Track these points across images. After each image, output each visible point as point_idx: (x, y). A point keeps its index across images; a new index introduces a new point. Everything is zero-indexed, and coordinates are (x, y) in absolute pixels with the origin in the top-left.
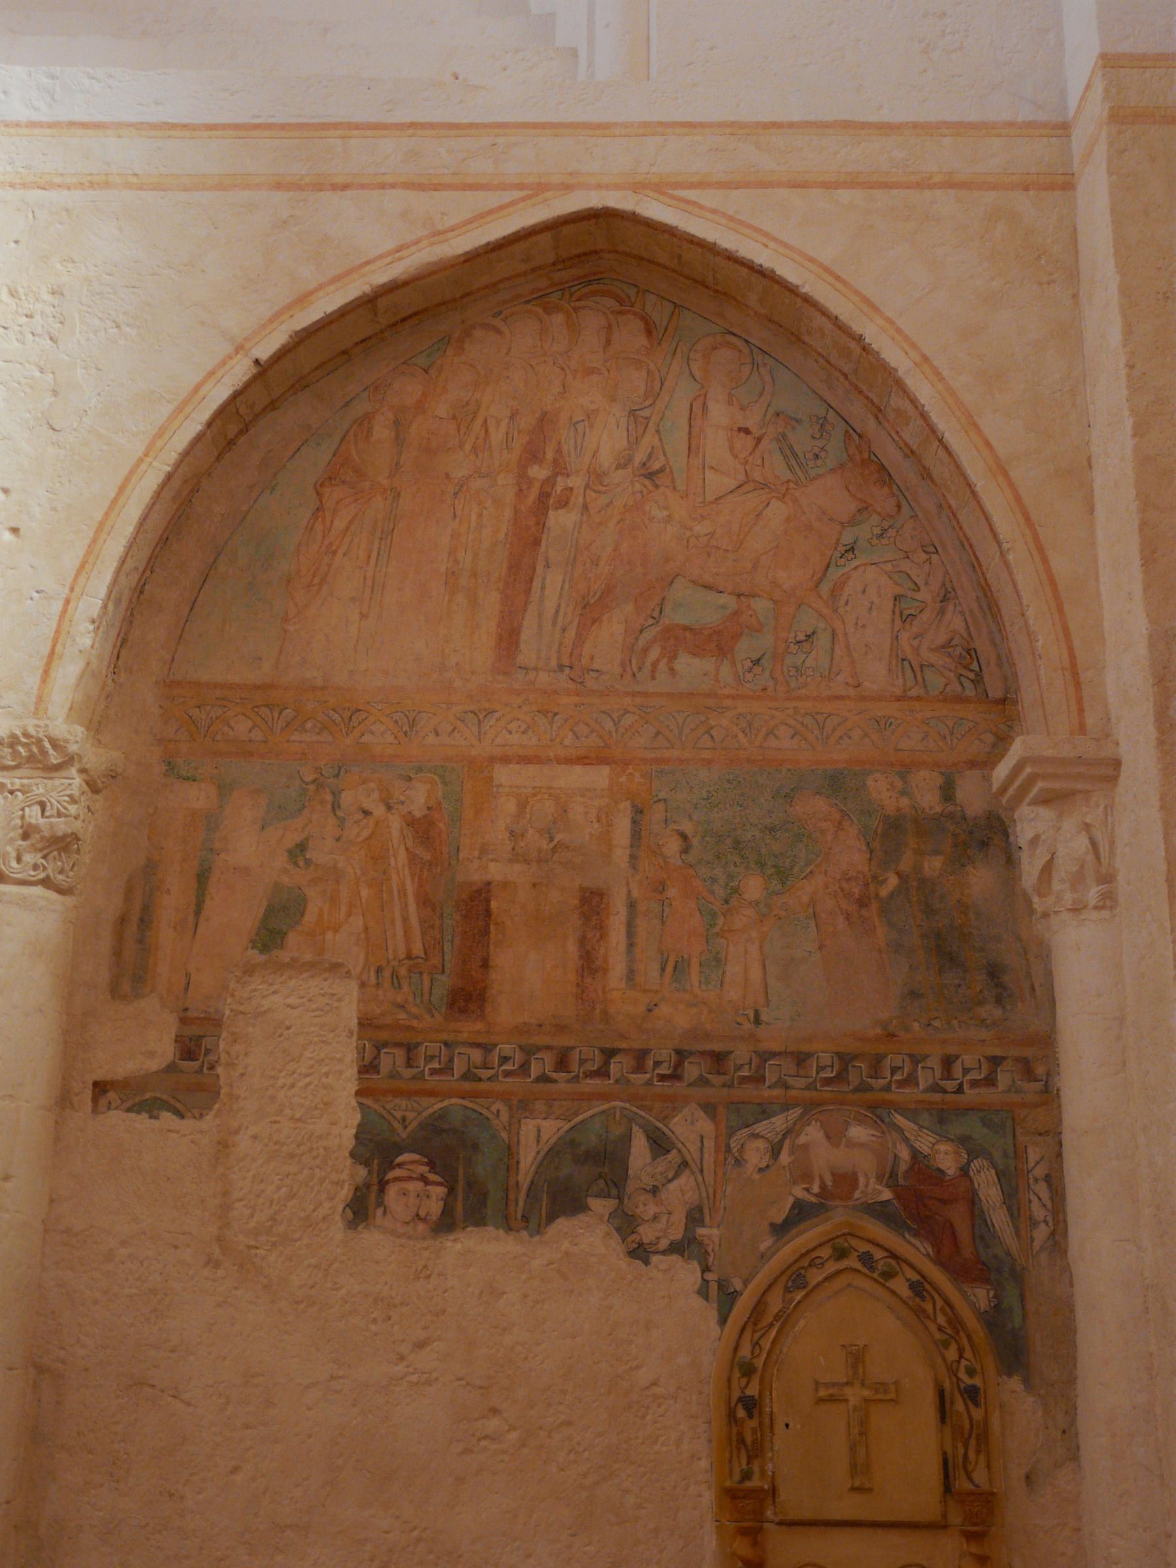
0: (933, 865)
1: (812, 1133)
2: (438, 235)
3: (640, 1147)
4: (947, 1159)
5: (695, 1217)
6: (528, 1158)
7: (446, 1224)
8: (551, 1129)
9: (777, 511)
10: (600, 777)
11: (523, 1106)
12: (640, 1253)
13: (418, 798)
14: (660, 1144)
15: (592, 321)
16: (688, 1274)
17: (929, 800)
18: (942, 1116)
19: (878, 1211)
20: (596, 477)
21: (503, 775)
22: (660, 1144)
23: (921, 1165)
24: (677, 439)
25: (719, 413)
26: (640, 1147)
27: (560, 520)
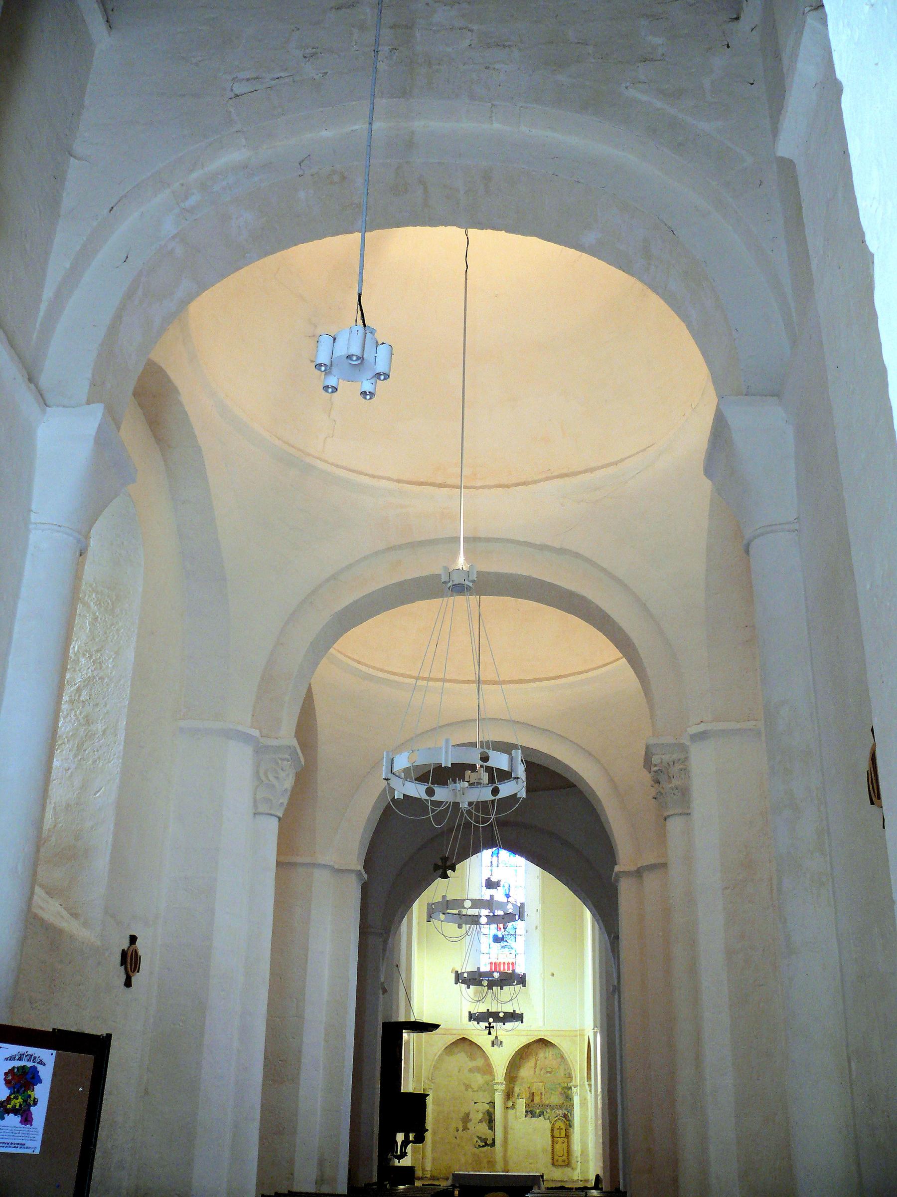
0: (566, 1091)
1: (557, 1111)
2: (529, 1040)
3: (545, 1112)
4: (566, 1113)
5: (549, 1117)
6: (537, 1113)
7: (532, 1117)
8: (539, 1110)
9: (555, 1061)
10: (542, 1084)
11: (536, 1109)
12: (545, 1119)
13: (528, 1085)
14: (546, 1112)
15: (540, 1044)
16: (549, 1121)
17: (566, 1085)
18: (566, 1109)
19: (561, 1116)
20: (541, 1058)
21: (535, 1084)
22: (546, 1112)
23: (564, 1113)
24: (547, 1055)
25: (551, 1053)
26: (545, 1112)
27: (538, 1062)
